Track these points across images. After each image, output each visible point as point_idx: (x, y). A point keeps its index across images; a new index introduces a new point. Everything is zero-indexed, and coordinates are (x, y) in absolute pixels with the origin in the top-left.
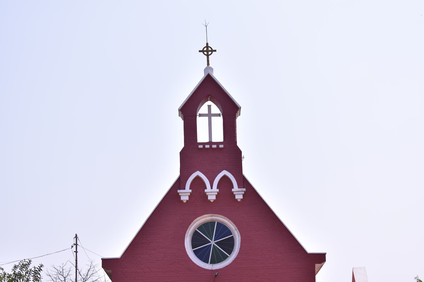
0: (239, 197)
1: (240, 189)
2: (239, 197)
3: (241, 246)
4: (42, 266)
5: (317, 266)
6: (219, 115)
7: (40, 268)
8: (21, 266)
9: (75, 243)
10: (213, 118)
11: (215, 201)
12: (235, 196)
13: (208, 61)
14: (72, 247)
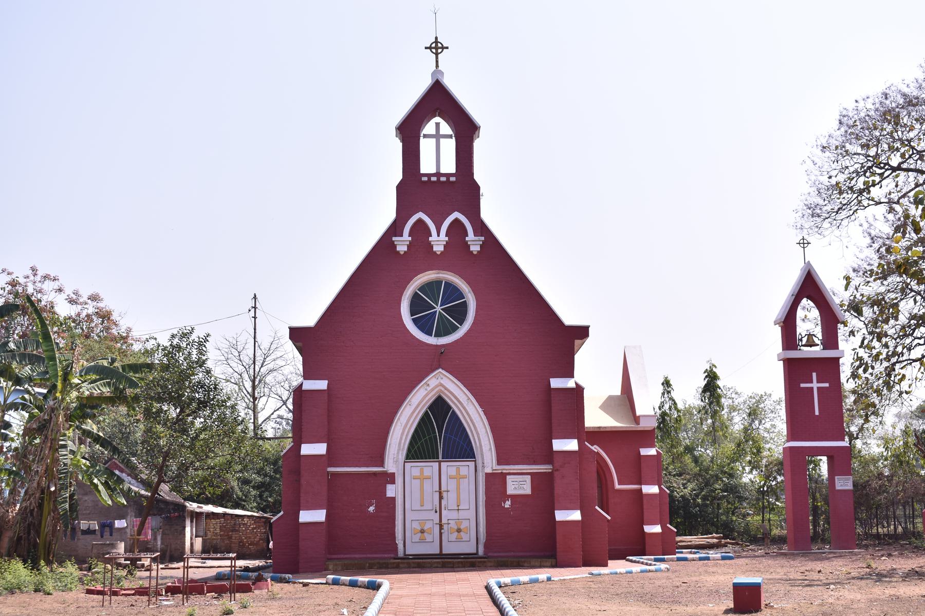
0: (475, 248)
1: (477, 238)
2: (475, 248)
4: (208, 335)
5: (577, 342)
6: (450, 136)
7: (206, 339)
8: (181, 336)
9: (254, 306)
10: (442, 140)
11: (442, 253)
12: (469, 246)
13: (437, 62)
14: (250, 311)
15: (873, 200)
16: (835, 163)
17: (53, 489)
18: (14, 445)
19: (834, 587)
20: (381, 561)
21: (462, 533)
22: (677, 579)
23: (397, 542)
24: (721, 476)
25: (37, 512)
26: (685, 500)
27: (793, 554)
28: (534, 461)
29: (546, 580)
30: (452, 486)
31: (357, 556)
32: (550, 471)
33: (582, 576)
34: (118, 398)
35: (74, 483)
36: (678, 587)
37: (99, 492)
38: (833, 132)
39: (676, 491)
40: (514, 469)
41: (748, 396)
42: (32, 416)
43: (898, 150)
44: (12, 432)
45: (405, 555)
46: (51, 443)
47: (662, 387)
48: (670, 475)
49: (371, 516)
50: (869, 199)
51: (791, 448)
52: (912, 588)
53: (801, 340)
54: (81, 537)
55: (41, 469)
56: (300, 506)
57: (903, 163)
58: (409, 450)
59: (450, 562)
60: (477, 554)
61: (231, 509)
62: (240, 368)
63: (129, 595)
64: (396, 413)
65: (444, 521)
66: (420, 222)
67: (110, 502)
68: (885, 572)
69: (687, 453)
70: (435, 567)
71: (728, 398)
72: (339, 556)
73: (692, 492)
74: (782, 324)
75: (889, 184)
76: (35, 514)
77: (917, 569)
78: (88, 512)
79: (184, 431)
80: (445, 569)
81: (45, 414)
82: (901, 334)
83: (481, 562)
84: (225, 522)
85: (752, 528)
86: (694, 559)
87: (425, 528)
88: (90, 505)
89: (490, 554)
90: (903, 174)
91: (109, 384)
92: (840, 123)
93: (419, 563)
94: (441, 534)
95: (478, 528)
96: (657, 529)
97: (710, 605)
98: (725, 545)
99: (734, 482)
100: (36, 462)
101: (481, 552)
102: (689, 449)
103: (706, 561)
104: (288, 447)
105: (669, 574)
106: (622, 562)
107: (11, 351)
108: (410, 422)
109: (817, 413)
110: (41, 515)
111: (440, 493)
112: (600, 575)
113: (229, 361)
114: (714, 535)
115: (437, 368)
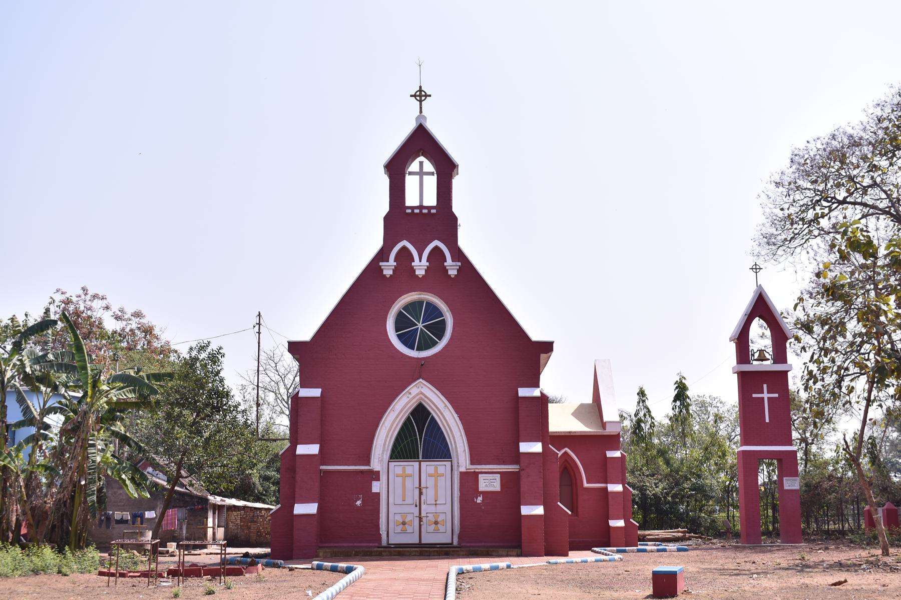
0: (453, 272)
1: (454, 263)
2: (453, 272)
5: (543, 356)
6: (432, 174)
7: (219, 351)
8: (199, 349)
9: (258, 323)
10: (425, 177)
11: (423, 276)
12: (447, 271)
13: (421, 108)
14: (254, 327)
15: (823, 230)
16: (788, 197)
17: (83, 483)
18: (54, 444)
19: (757, 576)
21: (439, 525)
23: (381, 533)
24: (690, 476)
25: (70, 503)
27: (744, 548)
28: (504, 462)
29: (505, 567)
31: (345, 545)
32: (517, 470)
33: (540, 564)
34: (143, 402)
35: (103, 478)
36: (619, 575)
37: (127, 486)
38: (786, 169)
39: (648, 490)
40: (485, 469)
42: (68, 419)
43: (843, 185)
44: (51, 432)
45: (388, 544)
46: (82, 443)
47: (638, 397)
48: (643, 475)
49: (358, 509)
50: (818, 229)
51: (743, 451)
52: (827, 578)
53: (754, 355)
54: (116, 526)
55: (73, 465)
56: (295, 501)
57: (847, 197)
58: (393, 451)
59: (426, 551)
60: (452, 544)
61: (253, 502)
63: (135, 577)
64: (381, 418)
65: (423, 514)
66: (404, 248)
67: (136, 496)
68: (812, 564)
69: (660, 456)
70: (413, 555)
73: (663, 490)
74: (736, 340)
75: (837, 215)
76: (68, 504)
77: (843, 562)
78: (123, 504)
79: (199, 433)
80: (422, 557)
81: (78, 417)
82: (848, 350)
83: (454, 551)
84: (245, 514)
85: (720, 523)
87: (407, 520)
88: (124, 498)
89: (463, 544)
90: (850, 206)
91: (134, 391)
92: (792, 162)
95: (453, 521)
96: (621, 523)
97: (637, 591)
98: (689, 539)
99: (701, 482)
100: (70, 459)
101: (455, 543)
102: (662, 453)
103: (663, 553)
104: (287, 447)
106: (589, 552)
107: (50, 361)
109: (767, 420)
110: (73, 507)
111: (420, 489)
112: (557, 563)
113: (267, 371)
114: (680, 529)
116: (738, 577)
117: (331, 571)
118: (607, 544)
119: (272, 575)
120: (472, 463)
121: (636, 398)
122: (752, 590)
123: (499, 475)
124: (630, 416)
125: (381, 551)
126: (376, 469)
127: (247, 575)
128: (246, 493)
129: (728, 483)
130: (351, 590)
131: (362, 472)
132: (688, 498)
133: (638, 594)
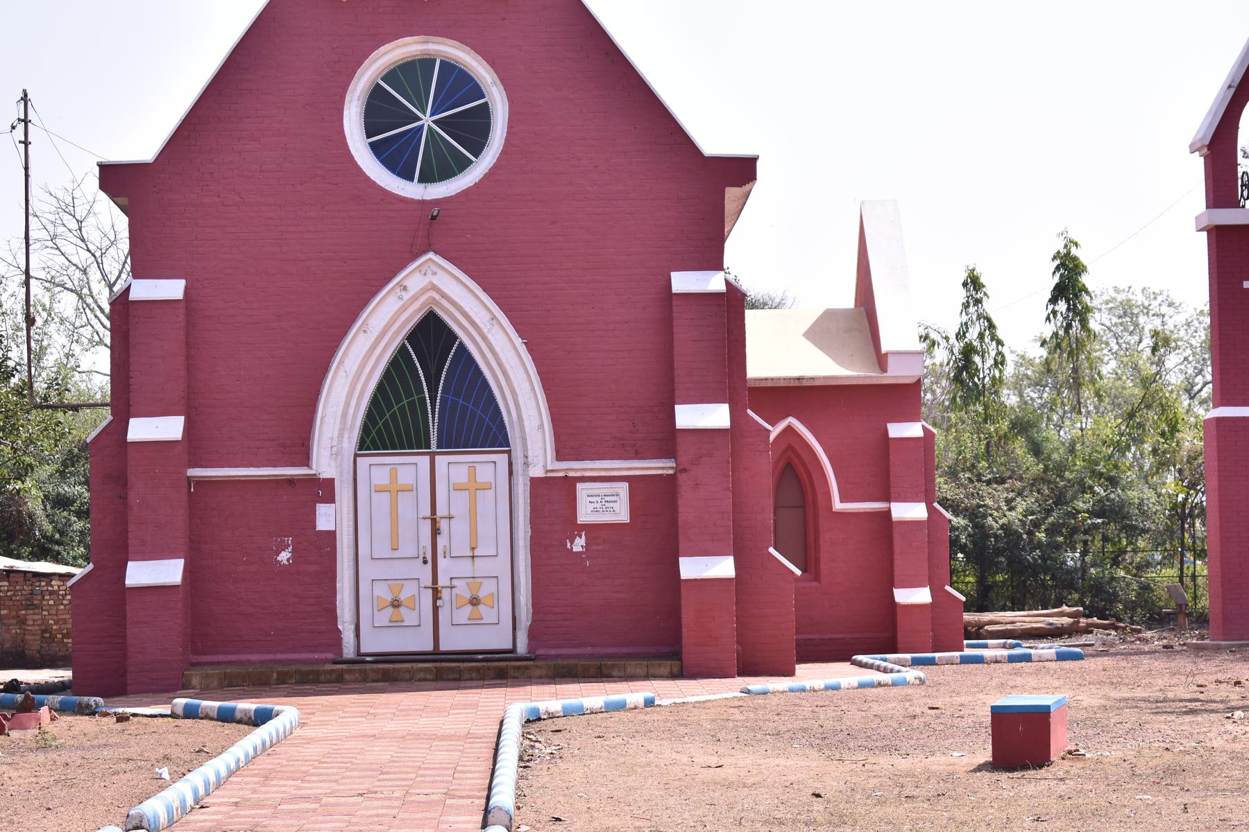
3: (508, 133)
5: (731, 193)
9: (23, 117)
14: (13, 128)
19: (1242, 714)
20: (304, 668)
21: (481, 607)
22: (922, 701)
23: (340, 627)
24: (1091, 482)
26: (1012, 535)
27: (1217, 649)
28: (637, 452)
29: (641, 703)
30: (460, 504)
31: (254, 657)
32: (671, 472)
33: (724, 696)
36: (915, 717)
40: (592, 470)
41: (1195, 309)
45: (359, 654)
48: (979, 480)
49: (284, 570)
51: (1219, 421)
58: (366, 430)
60: (513, 651)
61: (30, 560)
62: (83, 257)
65: (443, 581)
70: (420, 680)
71: (1153, 315)
72: (215, 658)
73: (1025, 516)
74: (1205, 150)
80: (440, 684)
83: (519, 668)
84: (11, 588)
85: (1161, 592)
86: (999, 659)
87: (402, 597)
89: (541, 651)
93: (385, 672)
94: (436, 609)
95: (516, 596)
96: (921, 595)
97: (956, 754)
98: (1087, 630)
99: (1118, 496)
101: (522, 648)
102: (1022, 426)
103: (1023, 664)
104: (105, 423)
105: (921, 691)
108: (367, 369)
112: (765, 693)
113: (58, 241)
114: (1065, 608)
115: (424, 252)
116: (1199, 718)
117: (217, 720)
118: (890, 646)
119: (75, 731)
120: (560, 456)
121: (961, 295)
122: (1228, 747)
123: (625, 485)
124: (947, 338)
125: (342, 672)
126: (323, 476)
127: (15, 734)
128: (11, 537)
129: (1181, 497)
130: (265, 763)
131: (290, 481)
132: (1086, 532)
133: (956, 760)
